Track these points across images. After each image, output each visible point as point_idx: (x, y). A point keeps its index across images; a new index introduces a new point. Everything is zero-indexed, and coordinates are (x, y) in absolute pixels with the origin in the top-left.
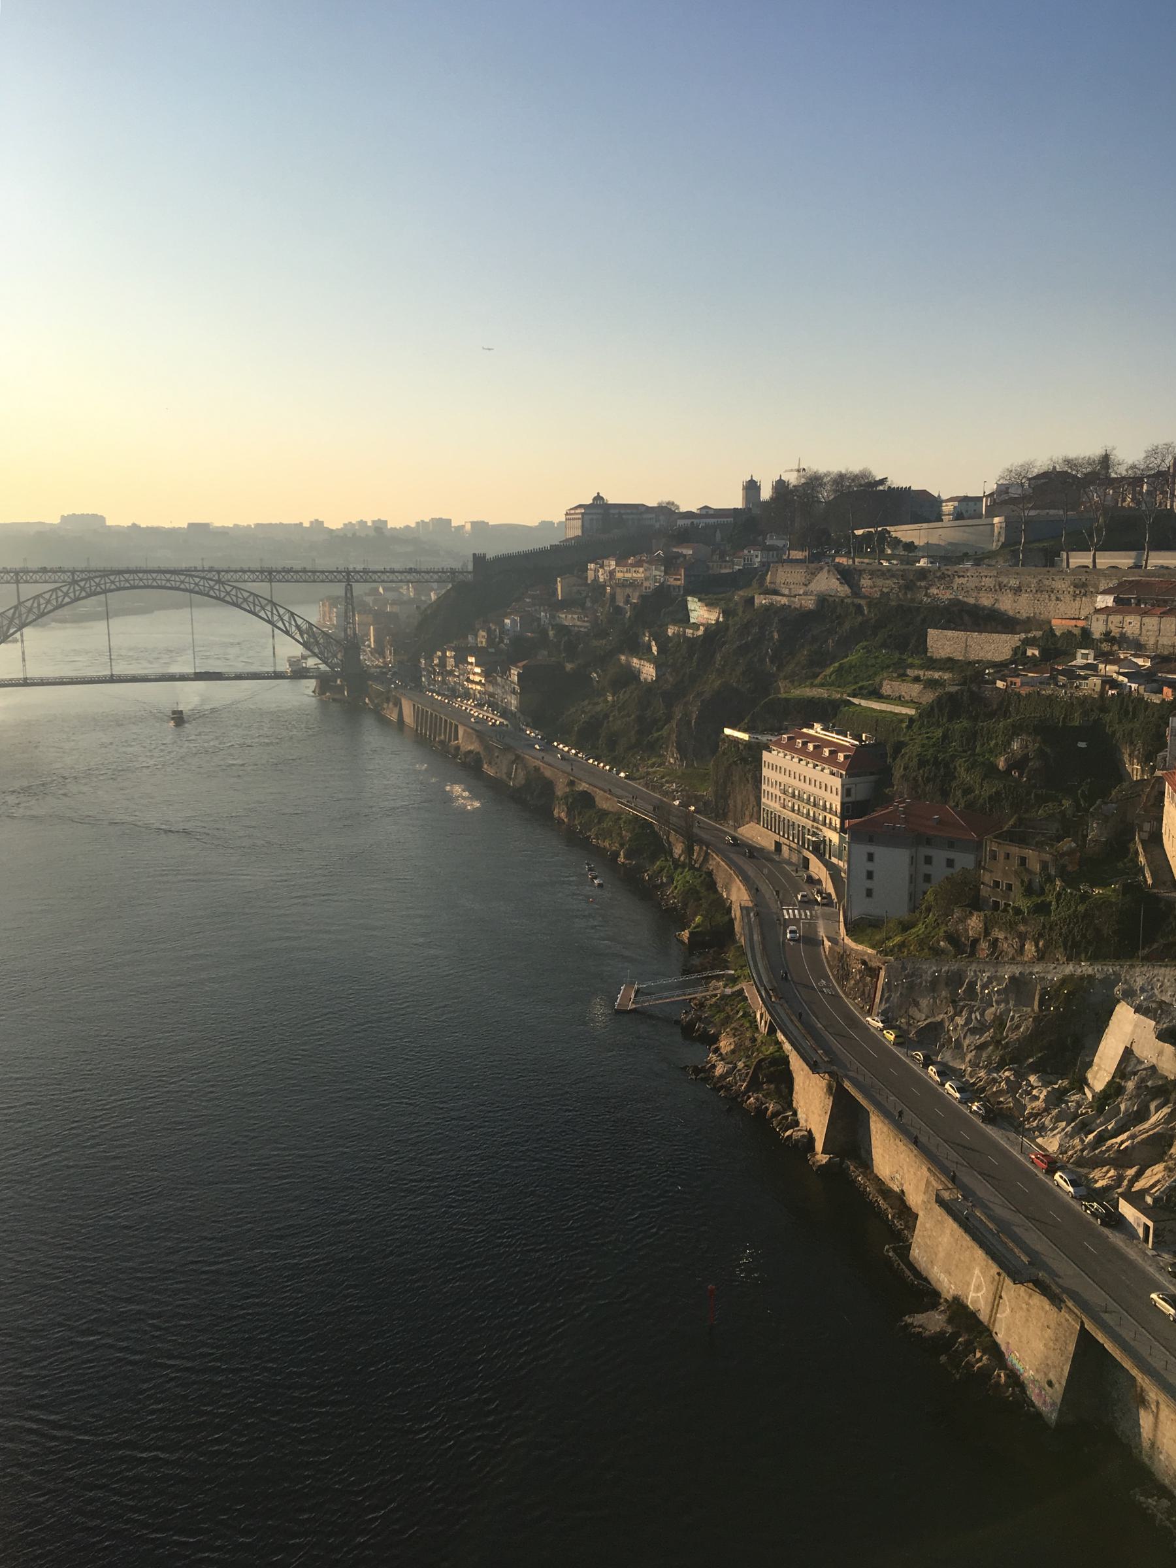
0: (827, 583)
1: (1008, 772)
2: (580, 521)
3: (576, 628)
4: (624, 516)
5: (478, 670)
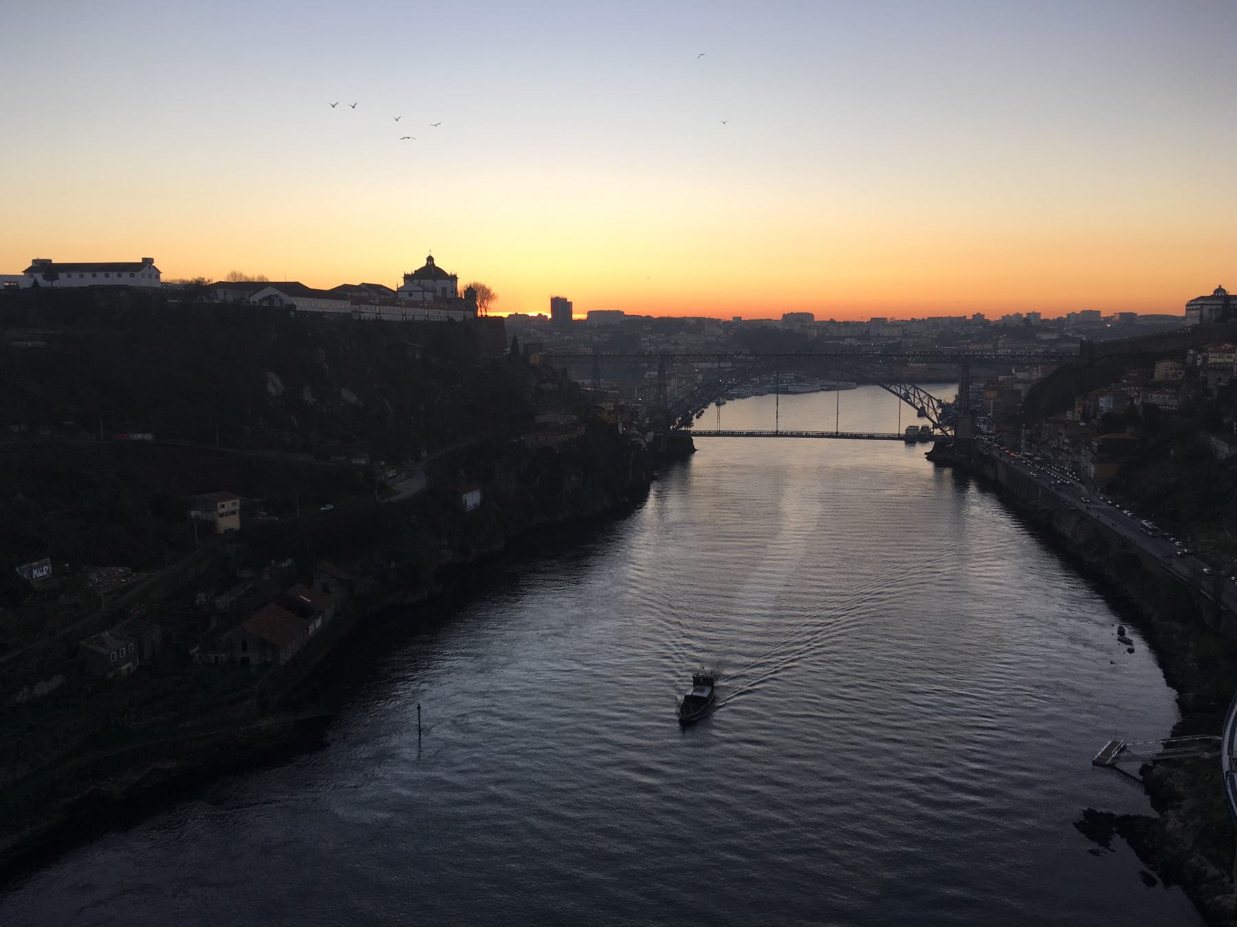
2: (1198, 313)
3: (1167, 407)
5: (1067, 441)
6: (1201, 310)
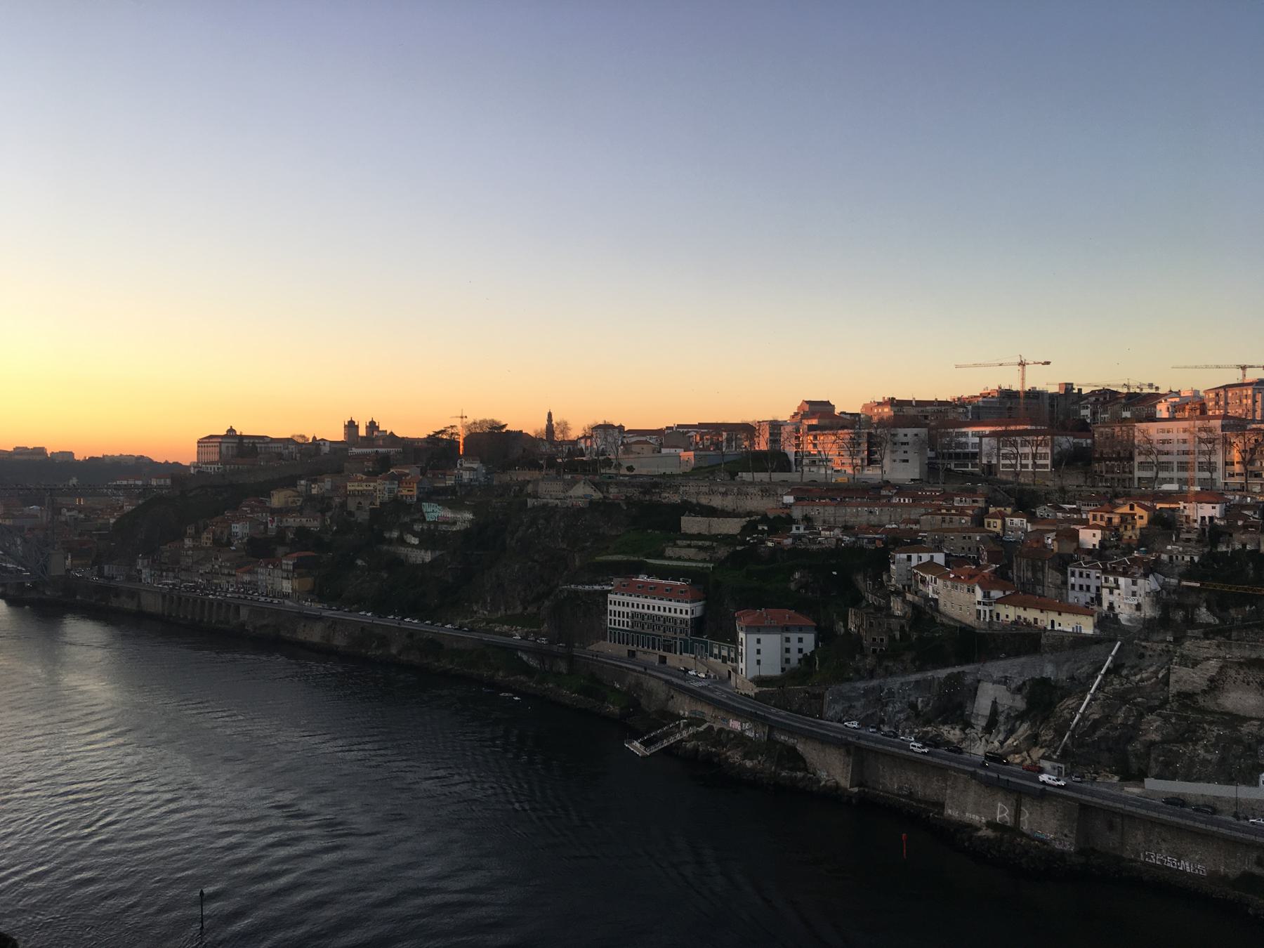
0: (582, 491)
2: (218, 449)
4: (258, 445)
6: (220, 449)
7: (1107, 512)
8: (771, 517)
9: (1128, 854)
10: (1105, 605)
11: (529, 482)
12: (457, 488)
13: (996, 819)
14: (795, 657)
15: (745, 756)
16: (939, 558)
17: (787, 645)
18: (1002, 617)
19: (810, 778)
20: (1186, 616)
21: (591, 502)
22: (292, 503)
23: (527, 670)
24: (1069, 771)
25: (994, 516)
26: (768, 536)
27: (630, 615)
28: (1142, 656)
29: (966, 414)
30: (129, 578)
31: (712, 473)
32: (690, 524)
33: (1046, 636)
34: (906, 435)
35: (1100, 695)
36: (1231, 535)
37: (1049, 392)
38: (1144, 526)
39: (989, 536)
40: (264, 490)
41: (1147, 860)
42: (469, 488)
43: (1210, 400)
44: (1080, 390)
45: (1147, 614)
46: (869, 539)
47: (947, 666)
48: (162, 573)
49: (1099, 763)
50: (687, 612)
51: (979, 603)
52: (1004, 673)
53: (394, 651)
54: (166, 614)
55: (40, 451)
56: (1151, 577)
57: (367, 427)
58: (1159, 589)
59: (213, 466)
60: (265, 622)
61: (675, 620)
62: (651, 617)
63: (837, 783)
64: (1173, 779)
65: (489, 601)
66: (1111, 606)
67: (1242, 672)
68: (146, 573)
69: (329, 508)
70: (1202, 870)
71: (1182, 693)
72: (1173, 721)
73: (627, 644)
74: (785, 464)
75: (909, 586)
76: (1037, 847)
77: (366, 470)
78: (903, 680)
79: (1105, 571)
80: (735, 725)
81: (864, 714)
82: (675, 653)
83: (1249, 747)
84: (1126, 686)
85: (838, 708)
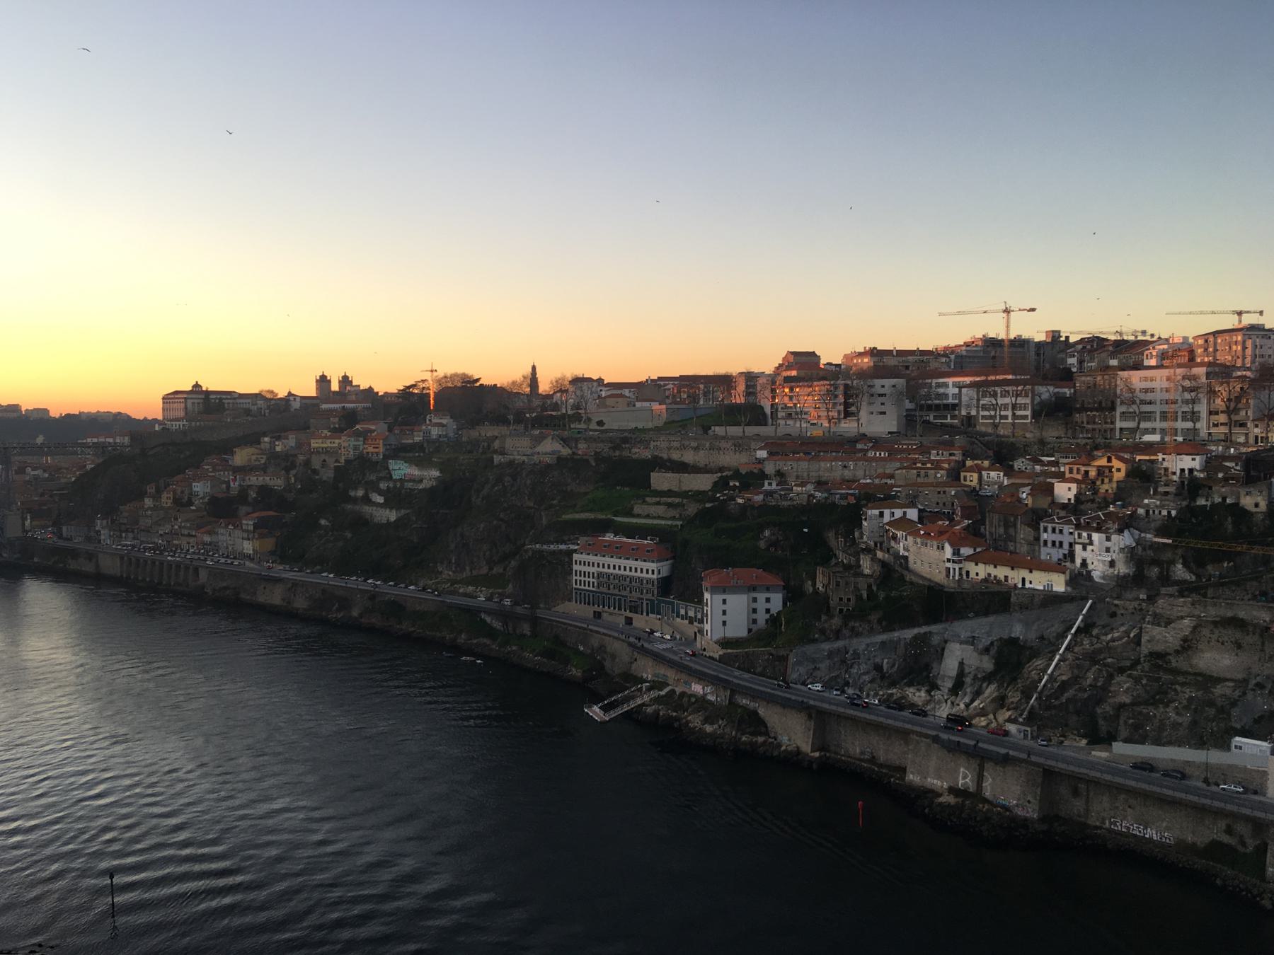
0: (550, 447)
1: (767, 549)
2: (183, 405)
6: (186, 403)
7: (1084, 465)
8: (744, 472)
9: (1093, 821)
10: (1078, 562)
11: (497, 437)
12: (425, 445)
13: (958, 785)
14: (762, 618)
15: (707, 720)
16: (913, 514)
17: (754, 605)
18: (972, 575)
19: (772, 743)
20: (1161, 573)
21: (559, 459)
22: (255, 461)
23: (491, 633)
24: (1035, 734)
25: (971, 470)
26: (740, 492)
27: (596, 575)
28: (1113, 615)
29: (948, 364)
30: (89, 539)
31: (684, 427)
32: (661, 480)
33: (1015, 594)
34: (883, 386)
35: (1069, 656)
36: (1210, 488)
37: (1036, 340)
38: (1122, 479)
39: (965, 491)
40: (227, 448)
41: (1112, 827)
42: (437, 444)
43: (1200, 346)
44: (1067, 338)
45: (1121, 571)
46: (841, 494)
47: (914, 626)
48: (121, 535)
49: (1066, 725)
50: (653, 573)
51: (949, 560)
52: (972, 632)
53: (355, 613)
54: (125, 576)
55: (14, 408)
56: (1126, 532)
57: (340, 381)
58: (1134, 545)
59: (178, 423)
60: (225, 584)
61: (641, 580)
62: (616, 577)
63: (798, 748)
64: (1143, 743)
65: (453, 561)
66: (1084, 563)
67: (1216, 631)
68: (104, 535)
69: (293, 466)
70: (1169, 837)
71: (1155, 653)
72: (1144, 682)
73: (593, 605)
74: (761, 417)
75: (881, 544)
76: (999, 813)
77: (332, 426)
78: (869, 641)
79: (1078, 526)
80: (697, 688)
81: (827, 677)
82: (642, 614)
83: (1221, 710)
84: (1095, 646)
85: (802, 670)
